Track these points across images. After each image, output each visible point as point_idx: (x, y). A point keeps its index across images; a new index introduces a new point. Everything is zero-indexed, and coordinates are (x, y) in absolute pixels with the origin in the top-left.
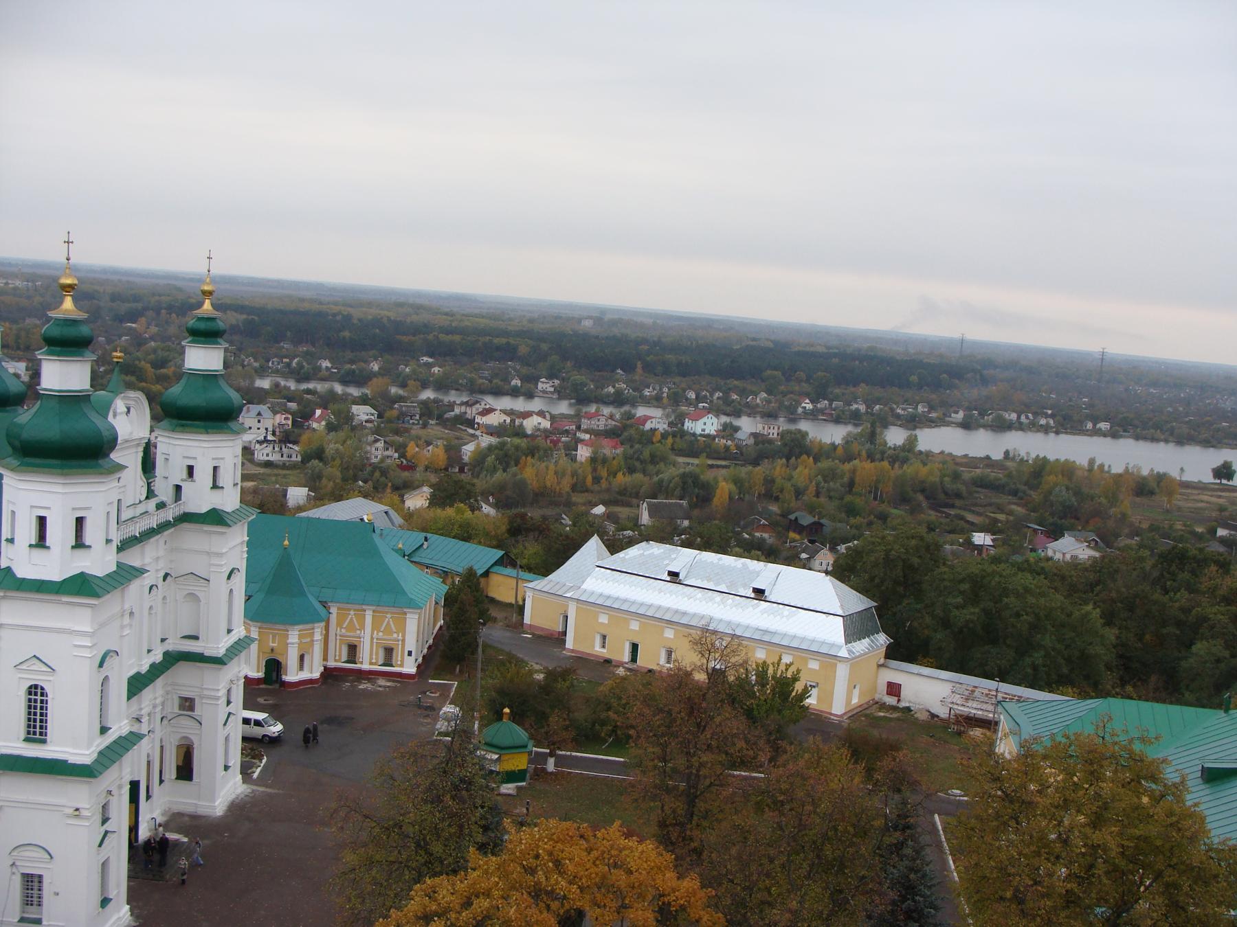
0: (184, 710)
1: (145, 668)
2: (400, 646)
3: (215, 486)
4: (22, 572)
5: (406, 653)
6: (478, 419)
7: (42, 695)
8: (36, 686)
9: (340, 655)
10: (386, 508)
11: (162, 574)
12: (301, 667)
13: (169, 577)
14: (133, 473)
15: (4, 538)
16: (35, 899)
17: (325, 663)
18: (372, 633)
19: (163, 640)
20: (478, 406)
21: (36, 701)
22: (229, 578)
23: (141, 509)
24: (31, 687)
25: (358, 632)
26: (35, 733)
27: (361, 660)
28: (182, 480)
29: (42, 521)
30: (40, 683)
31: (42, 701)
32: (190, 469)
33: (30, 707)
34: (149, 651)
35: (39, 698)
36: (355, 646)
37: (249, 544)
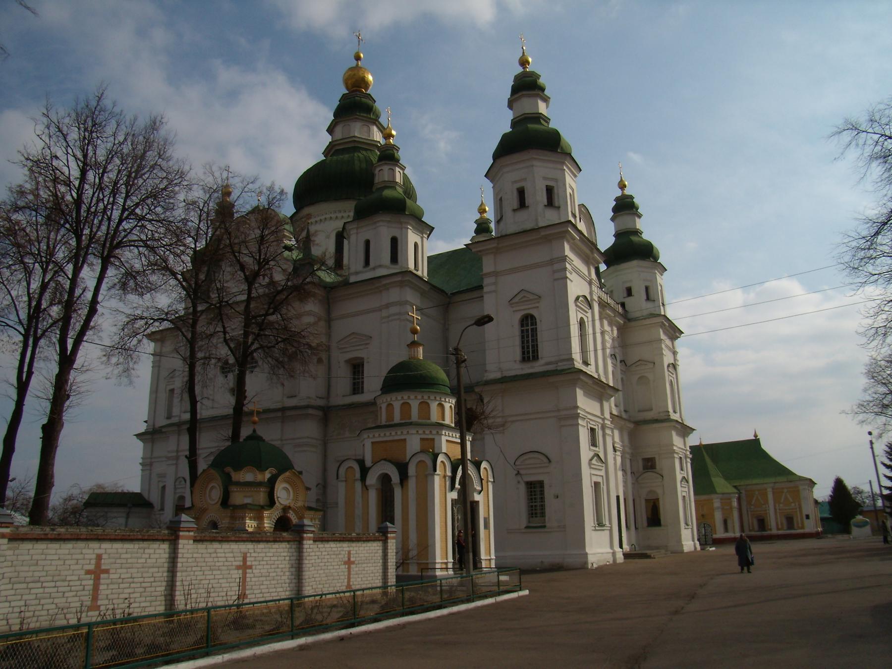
0: (647, 469)
2: (798, 512)
3: (648, 299)
5: (804, 517)
12: (726, 530)
16: (538, 511)
18: (775, 506)
21: (527, 330)
25: (764, 506)
26: (529, 358)
31: (532, 329)
35: (530, 327)
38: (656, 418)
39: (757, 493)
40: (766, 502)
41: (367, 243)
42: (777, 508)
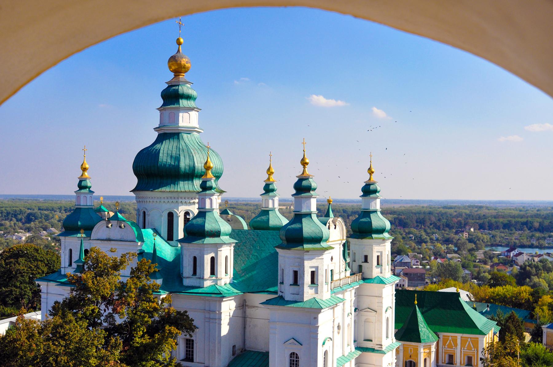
1: (346, 354)
2: (476, 355)
3: (378, 264)
4: (288, 297)
5: (479, 359)
6: (514, 259)
7: (296, 358)
8: (294, 353)
9: (445, 361)
10: (468, 293)
11: (353, 309)
13: (357, 310)
14: (337, 251)
15: (279, 282)
17: (437, 364)
18: (461, 349)
19: (355, 341)
20: (513, 252)
21: (294, 360)
22: (386, 311)
23: (343, 276)
24: (291, 354)
27: (455, 363)
28: (362, 262)
29: (296, 273)
30: (295, 352)
31: (296, 361)
32: (366, 257)
33: (291, 364)
34: (348, 345)
36: (453, 356)
37: (396, 295)
38: (373, 348)
39: (450, 338)
40: (456, 345)
41: (195, 258)
42: (462, 351)
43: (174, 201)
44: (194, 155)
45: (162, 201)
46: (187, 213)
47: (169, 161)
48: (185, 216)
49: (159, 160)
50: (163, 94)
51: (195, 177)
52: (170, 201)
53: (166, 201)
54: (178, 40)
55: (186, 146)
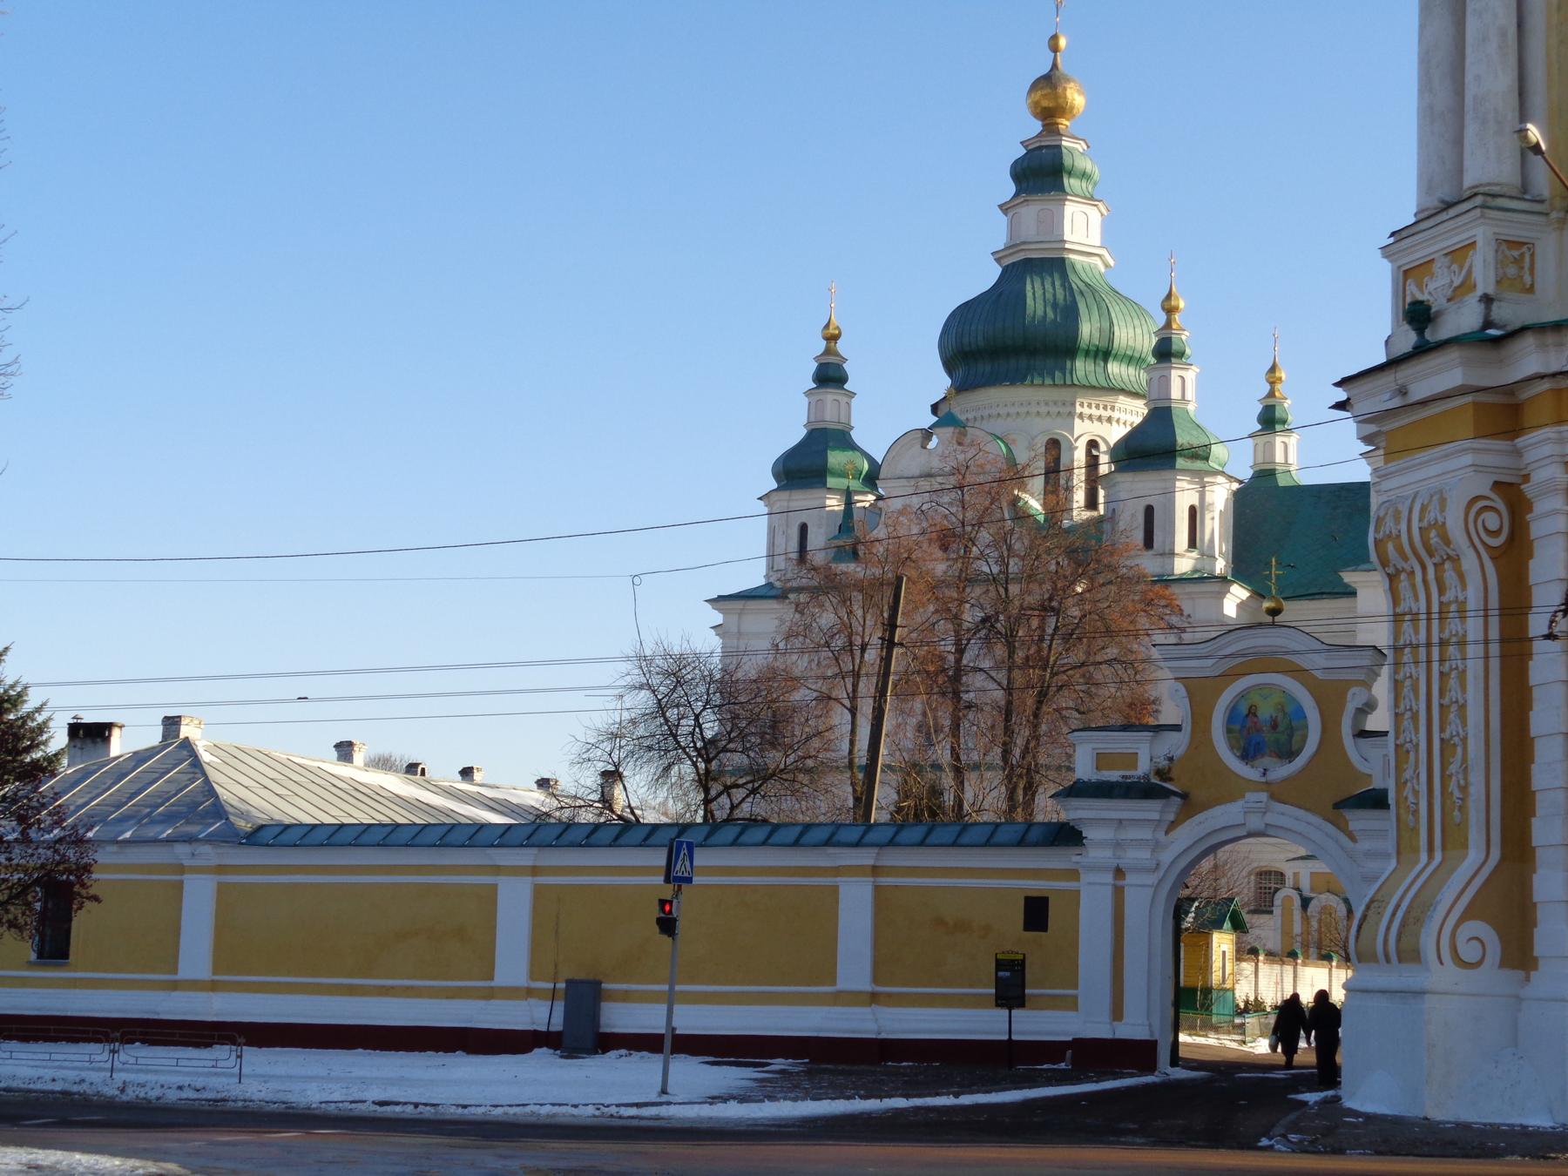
41: (1149, 511)
43: (1062, 410)
44: (1109, 305)
45: (1034, 410)
46: (1092, 444)
47: (1050, 314)
48: (1089, 453)
49: (1028, 312)
50: (1015, 168)
51: (1111, 359)
52: (1054, 410)
53: (1043, 409)
54: (1055, 38)
55: (1087, 285)
